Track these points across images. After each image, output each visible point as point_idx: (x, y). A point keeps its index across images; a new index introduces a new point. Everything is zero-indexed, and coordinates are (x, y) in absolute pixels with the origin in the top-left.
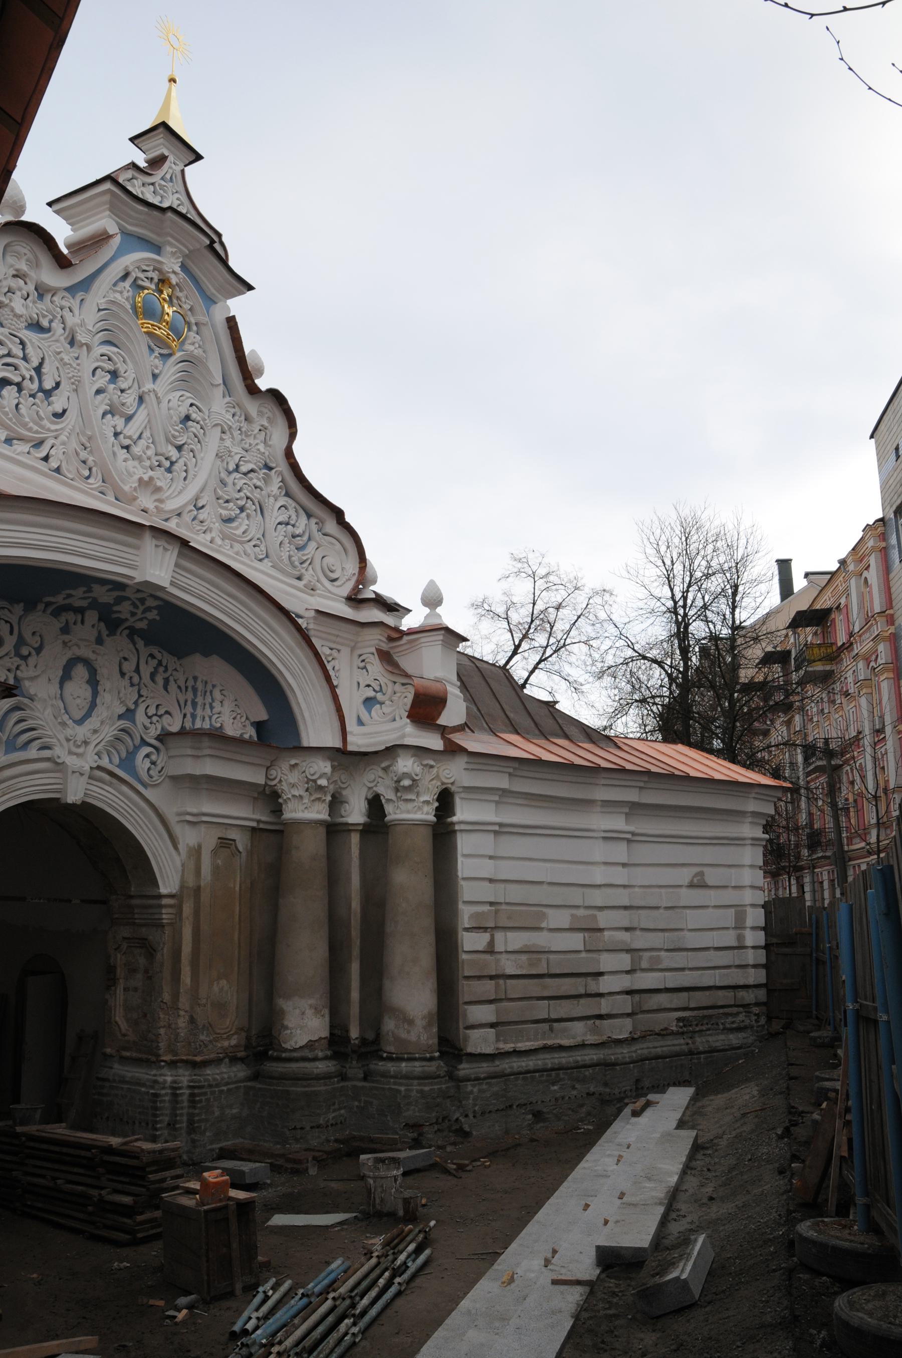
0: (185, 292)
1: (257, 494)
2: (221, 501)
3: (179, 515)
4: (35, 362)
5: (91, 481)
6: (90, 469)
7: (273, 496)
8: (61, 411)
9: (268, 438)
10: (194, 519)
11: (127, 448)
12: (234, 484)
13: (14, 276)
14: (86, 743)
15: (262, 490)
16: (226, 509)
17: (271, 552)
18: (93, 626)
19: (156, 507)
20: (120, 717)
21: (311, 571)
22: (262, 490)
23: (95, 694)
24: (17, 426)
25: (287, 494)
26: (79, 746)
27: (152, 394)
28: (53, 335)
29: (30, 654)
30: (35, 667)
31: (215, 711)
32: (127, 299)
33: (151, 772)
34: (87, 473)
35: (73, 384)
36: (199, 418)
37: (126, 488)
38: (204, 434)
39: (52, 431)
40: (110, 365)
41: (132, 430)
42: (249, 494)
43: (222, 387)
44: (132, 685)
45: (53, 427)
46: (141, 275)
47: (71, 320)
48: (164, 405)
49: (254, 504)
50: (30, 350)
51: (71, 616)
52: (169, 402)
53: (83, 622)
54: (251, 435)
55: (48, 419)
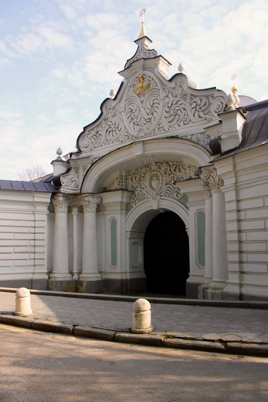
2: (168, 118)
3: (155, 130)
4: (114, 123)
10: (159, 128)
11: (138, 124)
12: (172, 110)
14: (157, 194)
15: (182, 104)
18: (155, 165)
20: (166, 184)
21: (210, 115)
22: (182, 104)
23: (160, 182)
26: (155, 195)
29: (142, 178)
30: (143, 181)
32: (132, 91)
33: (178, 196)
34: (127, 137)
36: (156, 102)
38: (159, 104)
41: (138, 120)
42: (177, 109)
44: (169, 175)
46: (134, 82)
49: (180, 110)
51: (150, 165)
53: (153, 166)
54: (176, 92)
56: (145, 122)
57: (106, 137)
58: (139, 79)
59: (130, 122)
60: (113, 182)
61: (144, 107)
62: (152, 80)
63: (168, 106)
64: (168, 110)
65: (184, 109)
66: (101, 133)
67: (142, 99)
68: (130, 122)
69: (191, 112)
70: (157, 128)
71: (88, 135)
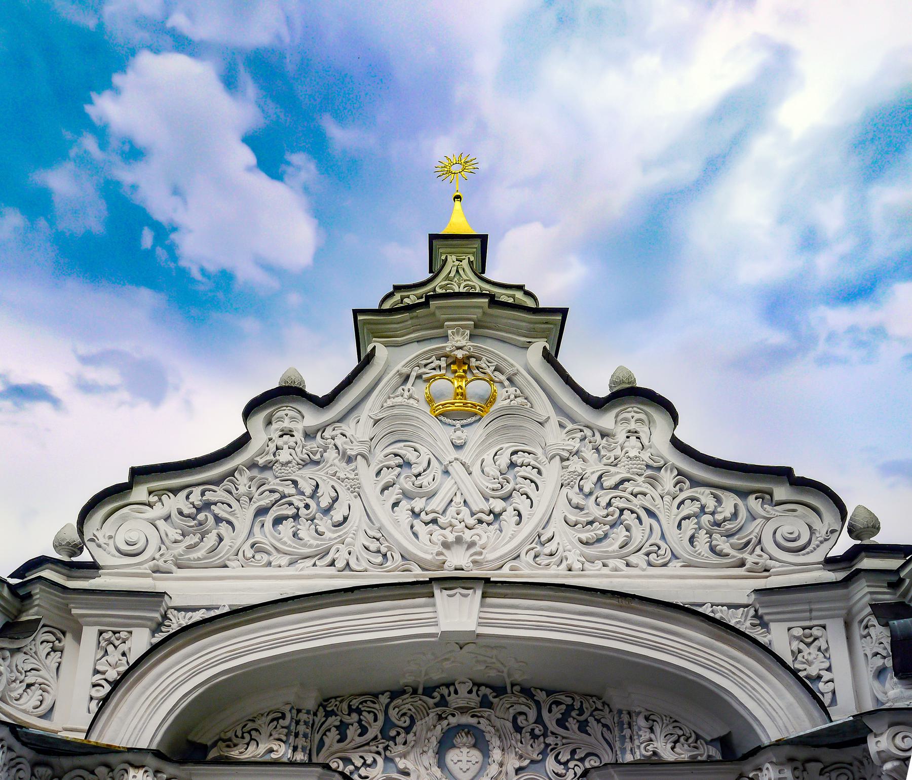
0: (484, 358)
1: (636, 503)
2: (580, 526)
4: (308, 491)
5: (389, 563)
6: (385, 556)
7: (668, 494)
8: (341, 519)
9: (645, 441)
10: (536, 557)
11: (434, 521)
13: (281, 436)
15: (645, 494)
16: (588, 531)
17: (679, 551)
19: (475, 562)
22: (645, 494)
24: (298, 549)
25: (695, 483)
27: (457, 466)
28: (327, 462)
31: (642, 739)
34: (379, 559)
35: (352, 492)
36: (526, 461)
37: (429, 557)
38: (539, 473)
39: (335, 538)
40: (396, 459)
41: (437, 503)
42: (622, 504)
43: (555, 419)
45: (336, 535)
46: (423, 370)
47: (340, 441)
48: (476, 469)
49: (633, 512)
50: (302, 484)
52: (483, 461)
55: (330, 531)
56: (471, 521)
57: (251, 533)
58: (448, 366)
59: (395, 504)
60: (250, 725)
61: (468, 461)
62: (507, 383)
63: (581, 489)
64: (577, 499)
65: (651, 514)
66: (223, 514)
67: (459, 433)
68: (395, 504)
69: (679, 526)
70: (532, 553)
71: (147, 508)
